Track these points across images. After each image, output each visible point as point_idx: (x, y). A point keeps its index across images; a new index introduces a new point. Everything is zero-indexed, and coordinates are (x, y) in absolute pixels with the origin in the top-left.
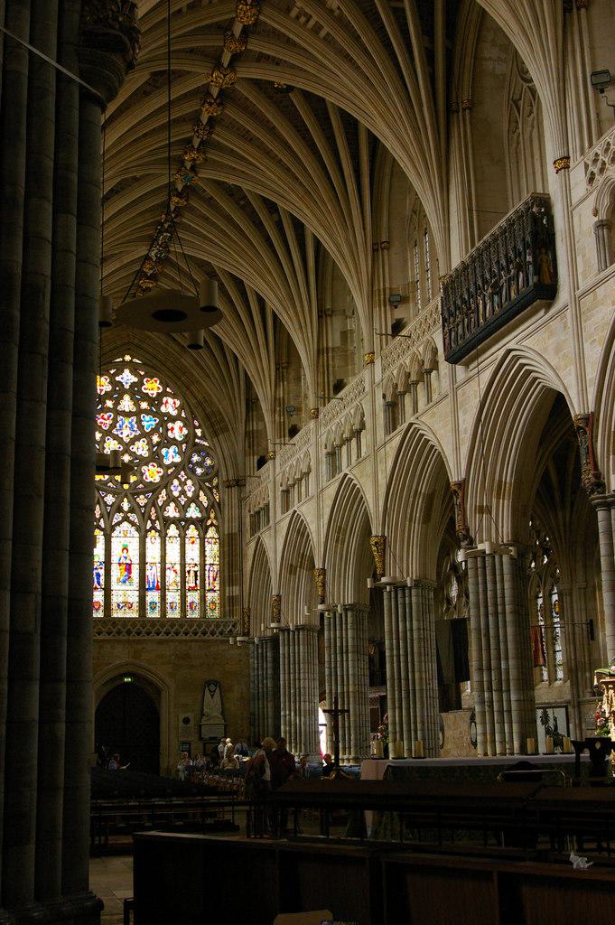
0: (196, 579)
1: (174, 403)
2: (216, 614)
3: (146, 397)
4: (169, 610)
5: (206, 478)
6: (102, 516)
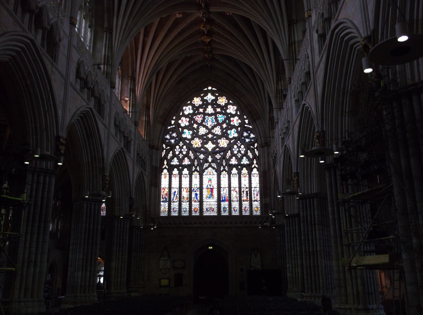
0: (247, 195)
1: (234, 108)
2: (258, 213)
3: (219, 106)
4: (233, 212)
5: (252, 143)
6: (198, 165)
